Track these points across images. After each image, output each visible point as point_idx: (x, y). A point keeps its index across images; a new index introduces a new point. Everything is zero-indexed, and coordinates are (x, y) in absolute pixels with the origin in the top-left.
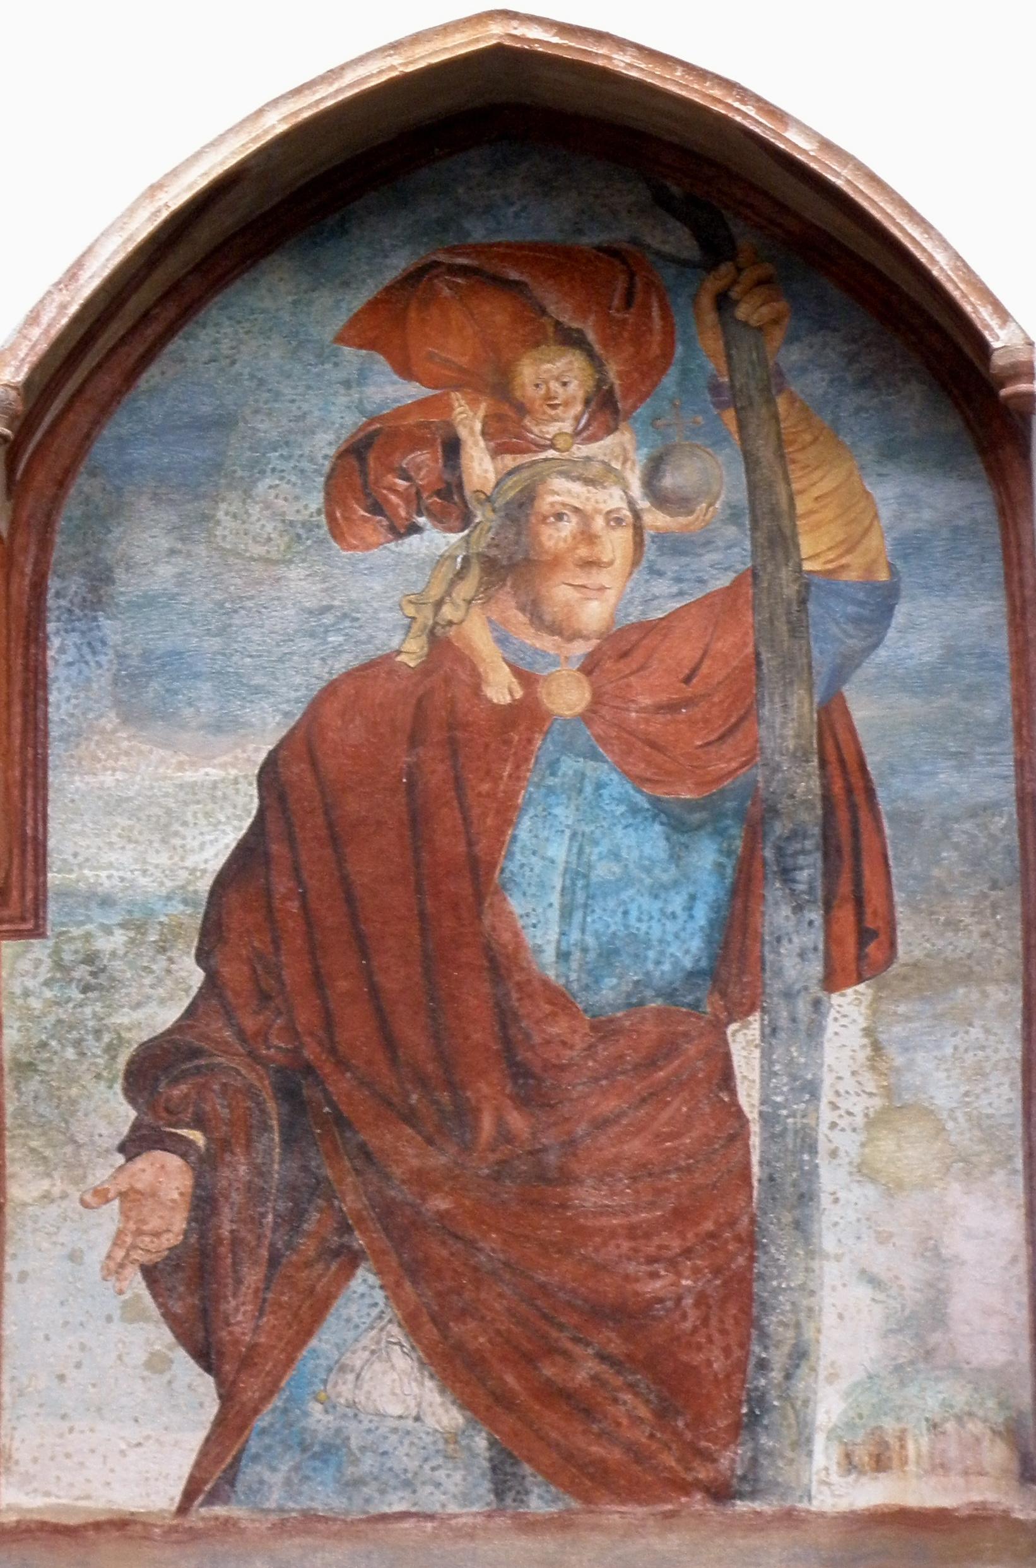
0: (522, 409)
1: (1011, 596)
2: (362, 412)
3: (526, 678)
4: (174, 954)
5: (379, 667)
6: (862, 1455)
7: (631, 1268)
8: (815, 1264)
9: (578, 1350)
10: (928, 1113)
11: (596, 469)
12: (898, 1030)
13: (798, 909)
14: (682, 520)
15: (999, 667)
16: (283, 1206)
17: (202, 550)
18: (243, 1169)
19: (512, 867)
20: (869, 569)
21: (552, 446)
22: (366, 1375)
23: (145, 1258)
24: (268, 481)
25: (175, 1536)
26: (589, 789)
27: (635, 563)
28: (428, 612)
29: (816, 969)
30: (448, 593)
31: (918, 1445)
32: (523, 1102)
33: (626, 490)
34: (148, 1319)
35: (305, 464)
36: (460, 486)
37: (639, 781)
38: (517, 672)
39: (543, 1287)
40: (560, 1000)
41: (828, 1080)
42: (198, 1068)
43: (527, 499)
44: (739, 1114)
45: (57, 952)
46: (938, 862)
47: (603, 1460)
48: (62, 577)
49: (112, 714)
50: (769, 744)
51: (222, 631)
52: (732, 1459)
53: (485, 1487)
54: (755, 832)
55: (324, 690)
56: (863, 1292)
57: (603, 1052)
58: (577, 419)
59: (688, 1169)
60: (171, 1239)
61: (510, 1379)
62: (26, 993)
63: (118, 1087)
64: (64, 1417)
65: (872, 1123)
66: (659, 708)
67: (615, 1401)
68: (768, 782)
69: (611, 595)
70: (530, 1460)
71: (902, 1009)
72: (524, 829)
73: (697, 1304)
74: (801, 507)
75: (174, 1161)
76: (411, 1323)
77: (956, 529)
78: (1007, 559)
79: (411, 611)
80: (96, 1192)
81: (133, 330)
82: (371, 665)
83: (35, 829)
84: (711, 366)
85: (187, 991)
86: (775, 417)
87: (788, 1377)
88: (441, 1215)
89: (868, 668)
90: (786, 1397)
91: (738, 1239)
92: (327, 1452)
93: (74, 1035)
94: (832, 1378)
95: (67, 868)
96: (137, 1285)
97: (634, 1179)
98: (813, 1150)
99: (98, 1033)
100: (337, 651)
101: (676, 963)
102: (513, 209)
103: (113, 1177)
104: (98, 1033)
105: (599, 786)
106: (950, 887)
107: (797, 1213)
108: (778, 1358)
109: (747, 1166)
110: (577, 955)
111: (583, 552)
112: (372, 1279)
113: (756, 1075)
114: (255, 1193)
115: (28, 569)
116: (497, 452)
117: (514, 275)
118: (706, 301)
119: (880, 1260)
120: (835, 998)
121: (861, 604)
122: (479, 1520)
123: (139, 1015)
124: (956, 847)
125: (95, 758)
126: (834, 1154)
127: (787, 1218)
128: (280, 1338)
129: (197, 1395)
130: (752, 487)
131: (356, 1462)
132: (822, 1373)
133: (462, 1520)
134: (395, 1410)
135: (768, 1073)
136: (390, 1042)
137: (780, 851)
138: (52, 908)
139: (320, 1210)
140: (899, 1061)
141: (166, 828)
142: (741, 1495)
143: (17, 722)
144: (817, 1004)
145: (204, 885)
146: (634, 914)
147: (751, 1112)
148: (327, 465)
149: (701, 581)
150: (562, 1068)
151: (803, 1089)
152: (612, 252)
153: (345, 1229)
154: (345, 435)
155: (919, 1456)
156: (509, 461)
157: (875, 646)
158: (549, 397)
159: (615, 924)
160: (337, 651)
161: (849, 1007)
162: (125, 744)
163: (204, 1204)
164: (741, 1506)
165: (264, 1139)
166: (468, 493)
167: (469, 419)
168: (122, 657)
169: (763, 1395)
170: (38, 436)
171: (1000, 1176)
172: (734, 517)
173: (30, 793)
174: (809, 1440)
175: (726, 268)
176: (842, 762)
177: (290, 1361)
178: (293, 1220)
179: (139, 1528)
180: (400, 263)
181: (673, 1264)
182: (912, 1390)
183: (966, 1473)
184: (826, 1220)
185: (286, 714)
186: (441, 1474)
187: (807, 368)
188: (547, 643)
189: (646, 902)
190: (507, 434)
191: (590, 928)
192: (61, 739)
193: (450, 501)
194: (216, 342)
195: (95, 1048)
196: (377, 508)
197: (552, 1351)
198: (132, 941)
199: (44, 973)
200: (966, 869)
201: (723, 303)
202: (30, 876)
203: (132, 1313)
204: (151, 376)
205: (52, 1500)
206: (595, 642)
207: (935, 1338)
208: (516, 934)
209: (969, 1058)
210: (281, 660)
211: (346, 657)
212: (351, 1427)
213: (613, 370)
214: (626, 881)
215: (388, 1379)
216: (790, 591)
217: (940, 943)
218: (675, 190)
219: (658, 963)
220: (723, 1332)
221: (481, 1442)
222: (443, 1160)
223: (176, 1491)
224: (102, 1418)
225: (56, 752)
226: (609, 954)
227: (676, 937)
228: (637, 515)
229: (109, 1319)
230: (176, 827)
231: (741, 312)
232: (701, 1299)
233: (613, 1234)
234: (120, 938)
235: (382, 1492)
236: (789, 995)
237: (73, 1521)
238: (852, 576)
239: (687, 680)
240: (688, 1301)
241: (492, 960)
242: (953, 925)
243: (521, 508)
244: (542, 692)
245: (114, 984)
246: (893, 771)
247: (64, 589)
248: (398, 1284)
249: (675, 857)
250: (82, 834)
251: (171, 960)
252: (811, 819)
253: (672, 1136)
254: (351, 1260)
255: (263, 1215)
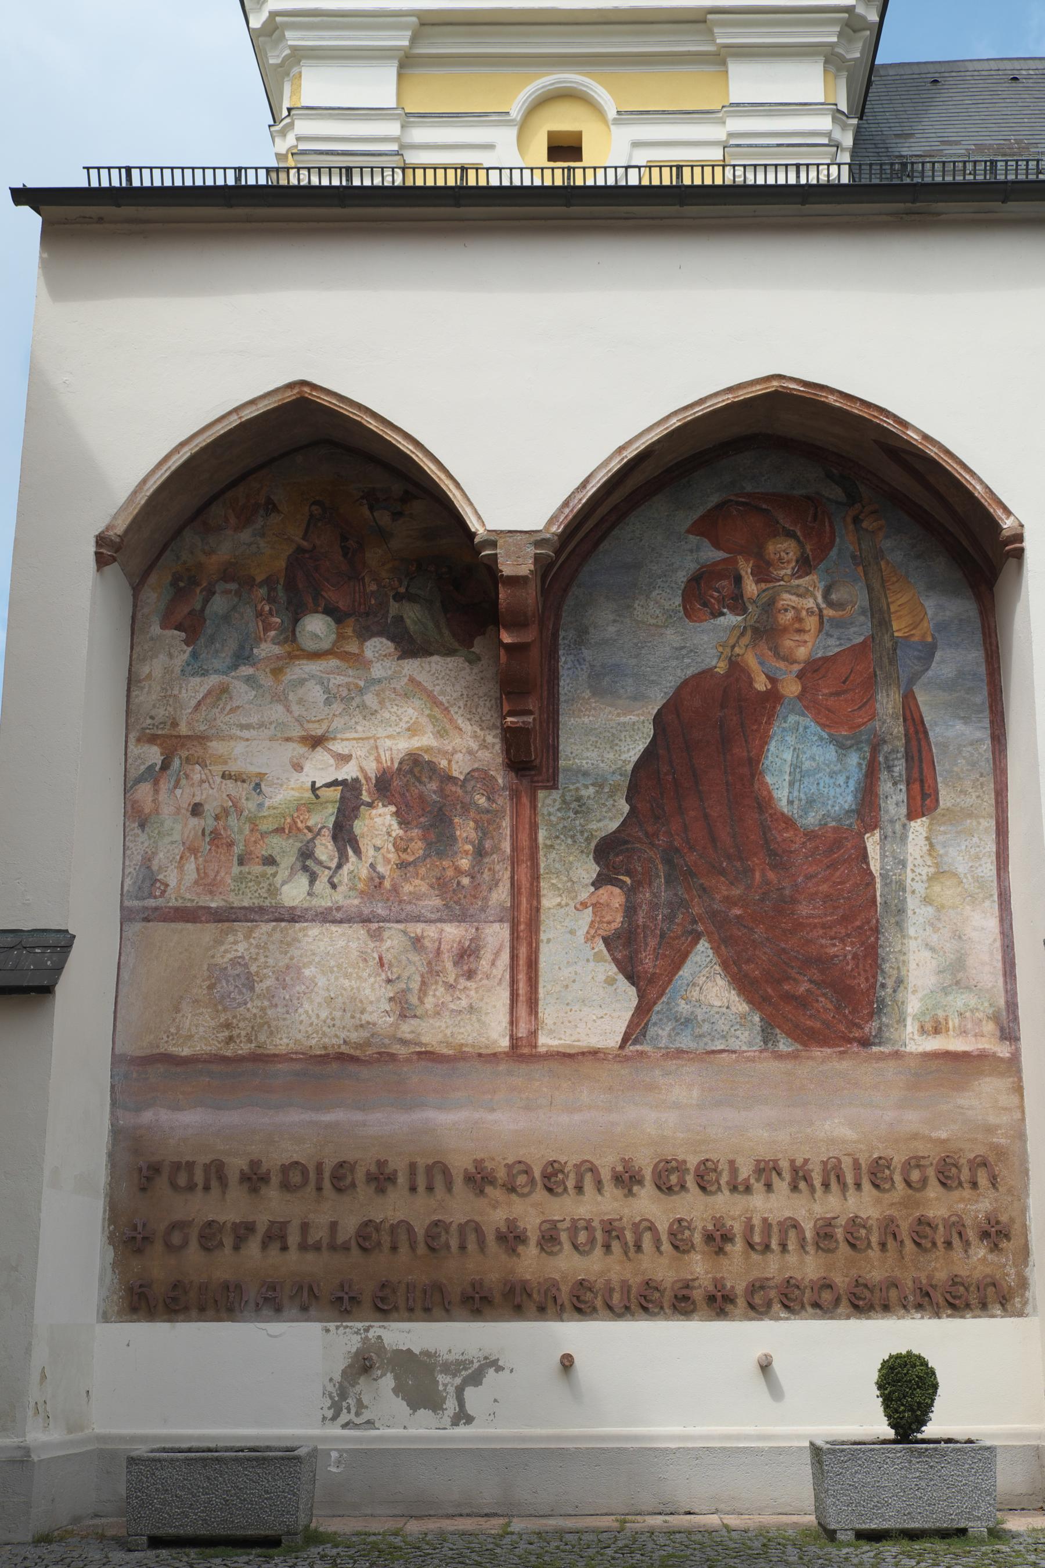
0: (769, 564)
1: (986, 650)
2: (698, 563)
3: (772, 680)
4: (616, 798)
5: (707, 674)
6: (928, 1027)
7: (823, 941)
8: (906, 941)
9: (800, 978)
10: (955, 875)
11: (801, 590)
12: (941, 838)
13: (895, 784)
14: (841, 613)
15: (982, 680)
16: (667, 911)
17: (628, 620)
18: (648, 895)
19: (767, 762)
20: (924, 636)
21: (782, 580)
22: (705, 988)
23: (604, 934)
24: (657, 592)
25: (618, 1059)
26: (801, 729)
27: (820, 631)
28: (728, 650)
29: (904, 810)
30: (737, 642)
31: (954, 1022)
32: (774, 867)
33: (815, 599)
34: (605, 961)
35: (673, 585)
36: (742, 596)
37: (823, 726)
38: (768, 677)
39: (783, 949)
40: (789, 822)
41: (910, 859)
42: (627, 849)
43: (772, 602)
44: (871, 874)
45: (563, 796)
46: (956, 765)
47: (813, 1028)
48: (566, 631)
49: (588, 692)
50: (880, 711)
51: (637, 656)
52: (871, 1027)
53: (759, 1039)
54: (875, 750)
55: (682, 683)
56: (928, 954)
57: (809, 845)
58: (793, 569)
59: (849, 898)
60: (616, 925)
61: (769, 990)
62: (550, 814)
63: (591, 857)
64: (568, 1004)
65: (931, 879)
66: (832, 694)
67: (817, 1001)
68: (881, 728)
69: (810, 644)
70: (779, 1027)
71: (942, 829)
72: (772, 746)
73: (853, 958)
74: (893, 608)
75: (617, 891)
76: (725, 965)
77: (961, 620)
78: (984, 633)
79: (721, 649)
80: (582, 903)
81: (596, 525)
82: (704, 672)
83: (553, 740)
84: (852, 548)
85: (622, 814)
86: (881, 570)
87: (895, 991)
88: (738, 917)
89: (924, 679)
90: (895, 1001)
91: (871, 929)
92: (687, 1022)
93: (571, 833)
94: (914, 992)
95: (567, 758)
96: (601, 946)
97: (825, 902)
98: (904, 890)
99: (582, 833)
100: (688, 666)
101: (841, 807)
102: (763, 479)
103: (590, 897)
104: (582, 833)
105: (806, 728)
106: (962, 775)
107: (897, 918)
108: (890, 983)
109: (875, 896)
110: (796, 802)
111: (797, 626)
112: (707, 945)
113: (878, 857)
114: (654, 906)
115: (551, 627)
116: (757, 582)
117: (764, 506)
118: (849, 520)
119: (934, 939)
120: (913, 824)
121: (920, 651)
122: (757, 1054)
123: (601, 825)
124: (964, 758)
125: (580, 711)
126: (913, 892)
127: (893, 920)
128: (665, 970)
129: (628, 996)
130: (871, 600)
131: (700, 1027)
132: (910, 990)
133: (748, 1054)
134: (718, 1003)
135: (883, 856)
136: (713, 839)
137: (886, 758)
138: (561, 776)
139: (683, 913)
140: (941, 852)
141: (612, 742)
142: (874, 1044)
143: (546, 693)
144: (904, 826)
145: (630, 768)
146: (822, 785)
147: (877, 874)
148: (683, 585)
149: (849, 639)
150: (791, 852)
151: (899, 863)
152: (808, 498)
153: (694, 922)
154: (691, 572)
155: (954, 1027)
156: (763, 586)
157: (927, 670)
158: (780, 559)
159: (814, 789)
160: (688, 666)
161: (918, 828)
162: (593, 705)
163: (630, 910)
164: (875, 1049)
165: (658, 881)
166: (745, 599)
167: (745, 568)
168: (592, 666)
169: (883, 999)
170: (555, 570)
171: (987, 903)
172: (863, 613)
173: (551, 725)
174: (904, 1020)
175: (858, 506)
176: (913, 720)
177: (670, 981)
178: (670, 918)
179: (602, 1055)
180: (714, 500)
181: (842, 940)
182: (950, 998)
183: (976, 1035)
184: (910, 922)
185: (665, 693)
186: (738, 1033)
187: (894, 550)
188: (782, 665)
189: (827, 779)
190: (762, 574)
191: (802, 791)
192: (565, 701)
193: (737, 602)
194: (633, 531)
195: (580, 839)
196: (705, 604)
197: (788, 978)
198: (597, 792)
199: (557, 805)
200: (969, 768)
201: (856, 520)
202: (551, 762)
203: (598, 958)
204: (605, 545)
205: (562, 1042)
206: (802, 665)
207: (960, 975)
208: (769, 792)
209: (973, 851)
210: (663, 669)
211: (692, 669)
212: (698, 1011)
213: (808, 547)
214: (818, 769)
215: (714, 990)
216: (889, 645)
217: (958, 800)
218: (835, 471)
219: (833, 806)
220: (865, 971)
221: (757, 1019)
222: (738, 892)
223: (619, 1039)
224: (585, 1005)
225: (563, 707)
226: (811, 802)
227: (840, 796)
228: (820, 610)
229: (588, 960)
230: (617, 741)
231: (865, 524)
232: (855, 956)
233: (815, 926)
234: (591, 790)
235: (712, 1040)
236: (892, 822)
237: (573, 1051)
238: (916, 639)
239: (844, 682)
240: (849, 957)
241: (758, 803)
242: (963, 792)
243: (770, 606)
244: (780, 687)
245: (589, 810)
246: (936, 724)
247: (566, 636)
248: (719, 947)
249: (840, 760)
250: (575, 744)
251: (614, 801)
252: (900, 744)
253: (842, 883)
254: (697, 937)
255: (657, 915)
